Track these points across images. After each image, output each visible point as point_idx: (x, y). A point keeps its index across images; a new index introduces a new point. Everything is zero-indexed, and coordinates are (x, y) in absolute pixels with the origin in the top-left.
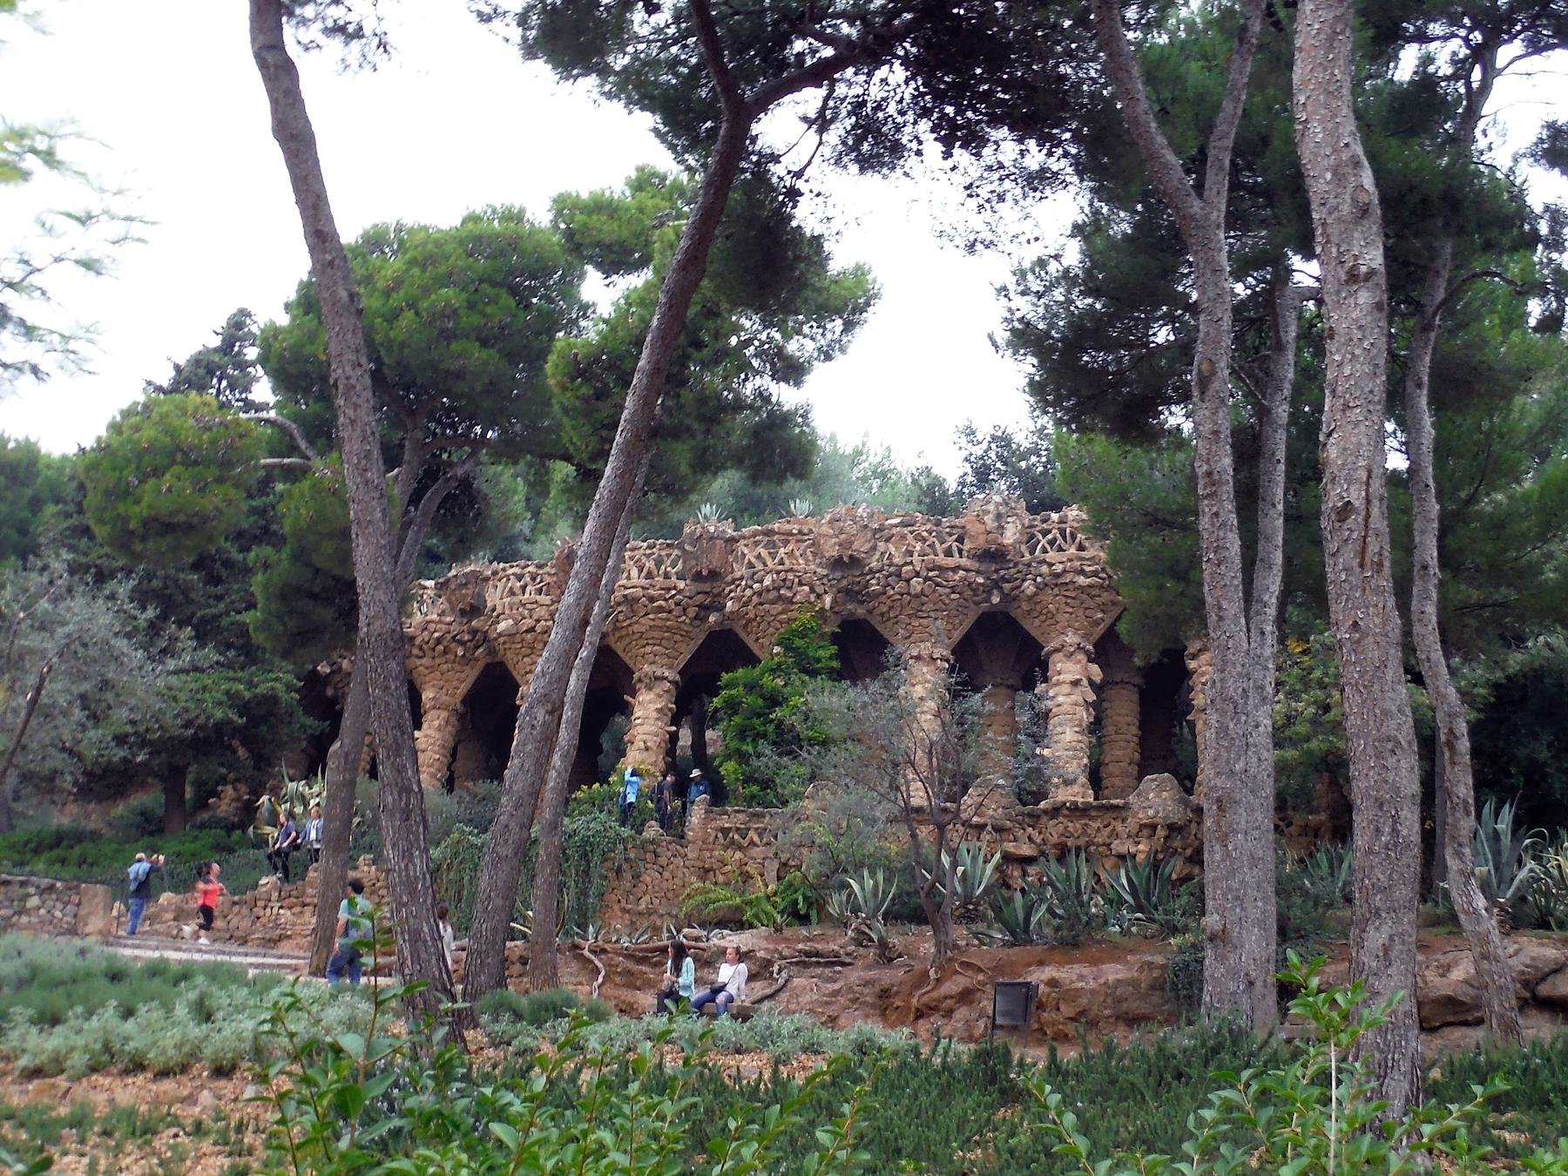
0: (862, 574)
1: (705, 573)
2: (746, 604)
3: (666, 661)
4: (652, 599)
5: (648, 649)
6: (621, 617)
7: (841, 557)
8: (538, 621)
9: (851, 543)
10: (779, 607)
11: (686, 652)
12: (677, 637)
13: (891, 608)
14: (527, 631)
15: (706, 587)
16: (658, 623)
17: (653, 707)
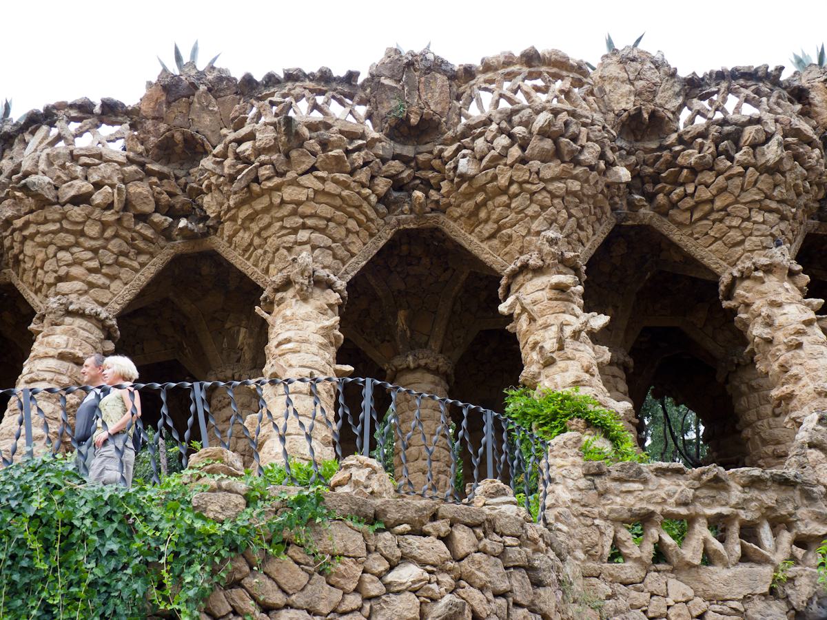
0: (662, 148)
1: (414, 120)
2: (495, 161)
3: (329, 260)
4: (325, 145)
5: (303, 235)
6: (265, 172)
7: (639, 111)
8: (98, 186)
9: (654, 93)
10: (554, 168)
11: (362, 251)
12: (352, 224)
13: (722, 190)
14: (78, 200)
15: (408, 151)
16: (330, 187)
17: (313, 326)
